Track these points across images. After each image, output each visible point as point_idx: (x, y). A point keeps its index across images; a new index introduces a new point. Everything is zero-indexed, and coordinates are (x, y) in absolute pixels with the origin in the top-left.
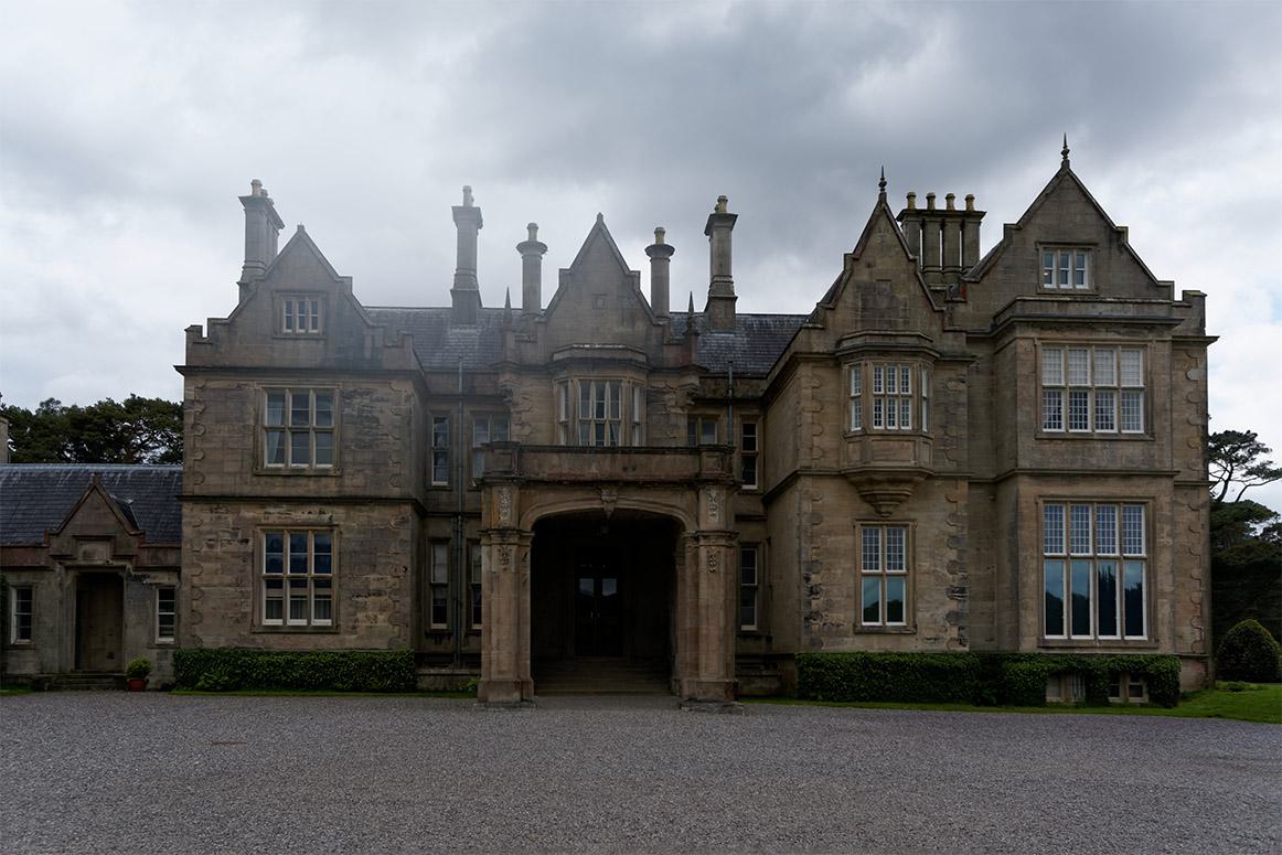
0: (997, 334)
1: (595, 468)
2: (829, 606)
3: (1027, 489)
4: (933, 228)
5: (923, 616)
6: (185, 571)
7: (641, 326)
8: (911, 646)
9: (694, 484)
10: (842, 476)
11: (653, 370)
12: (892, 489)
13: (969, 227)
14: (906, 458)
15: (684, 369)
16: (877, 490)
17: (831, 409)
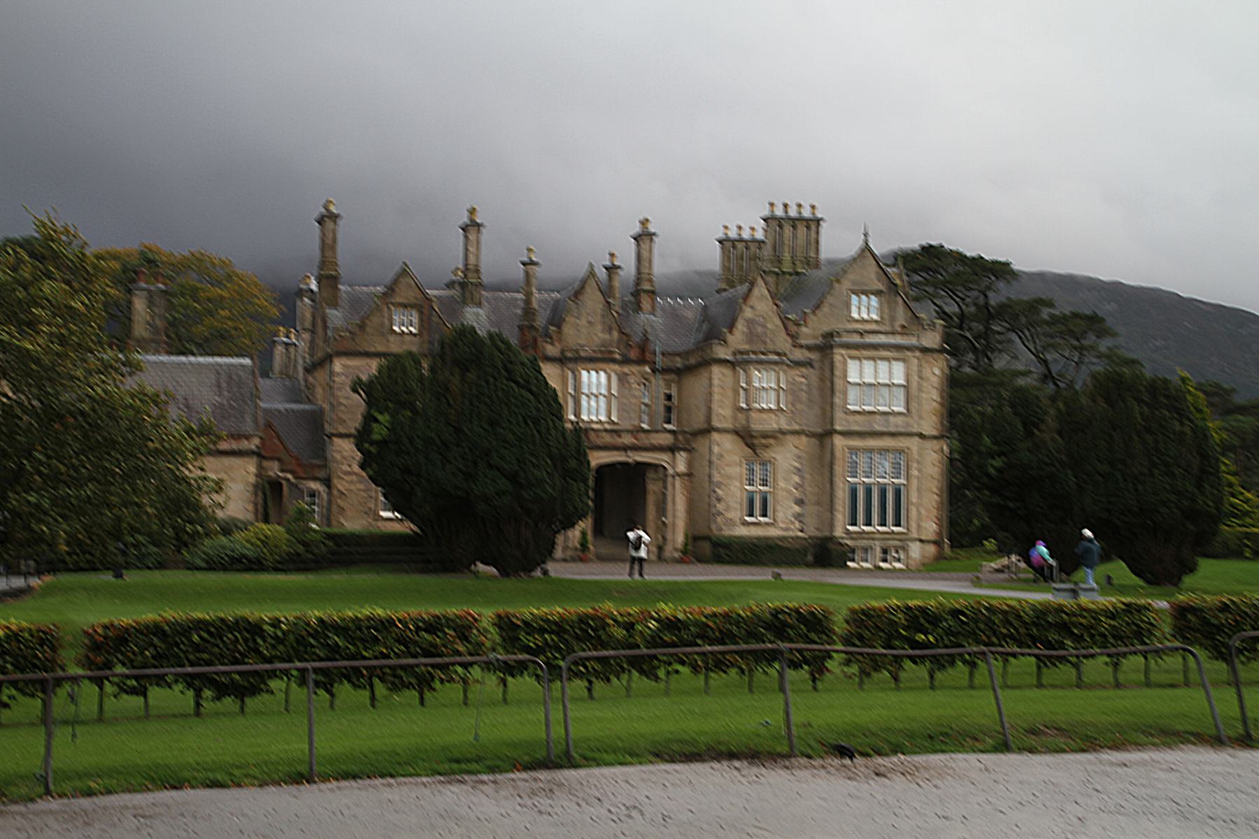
0: (826, 345)
1: (627, 440)
2: (728, 509)
3: (839, 441)
4: (788, 230)
5: (780, 515)
6: (335, 481)
7: (615, 334)
8: (773, 532)
9: (672, 449)
10: (736, 432)
11: (626, 361)
12: (763, 441)
13: (813, 227)
14: (772, 423)
15: (641, 361)
16: (756, 442)
17: (730, 393)
